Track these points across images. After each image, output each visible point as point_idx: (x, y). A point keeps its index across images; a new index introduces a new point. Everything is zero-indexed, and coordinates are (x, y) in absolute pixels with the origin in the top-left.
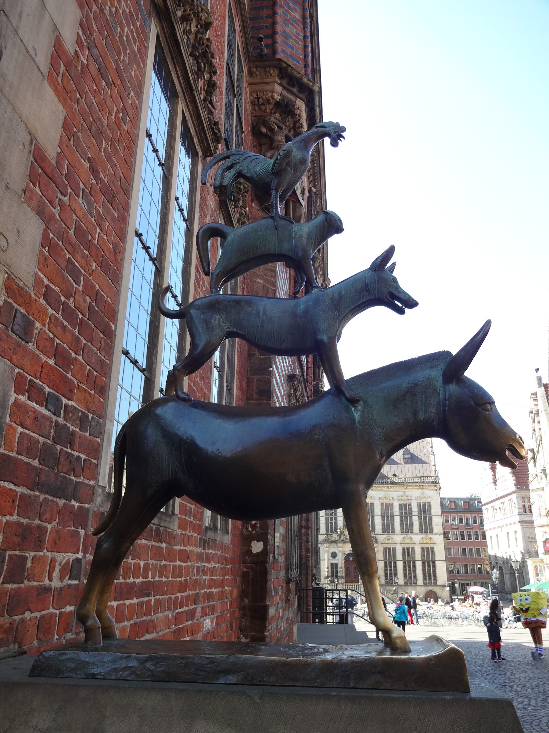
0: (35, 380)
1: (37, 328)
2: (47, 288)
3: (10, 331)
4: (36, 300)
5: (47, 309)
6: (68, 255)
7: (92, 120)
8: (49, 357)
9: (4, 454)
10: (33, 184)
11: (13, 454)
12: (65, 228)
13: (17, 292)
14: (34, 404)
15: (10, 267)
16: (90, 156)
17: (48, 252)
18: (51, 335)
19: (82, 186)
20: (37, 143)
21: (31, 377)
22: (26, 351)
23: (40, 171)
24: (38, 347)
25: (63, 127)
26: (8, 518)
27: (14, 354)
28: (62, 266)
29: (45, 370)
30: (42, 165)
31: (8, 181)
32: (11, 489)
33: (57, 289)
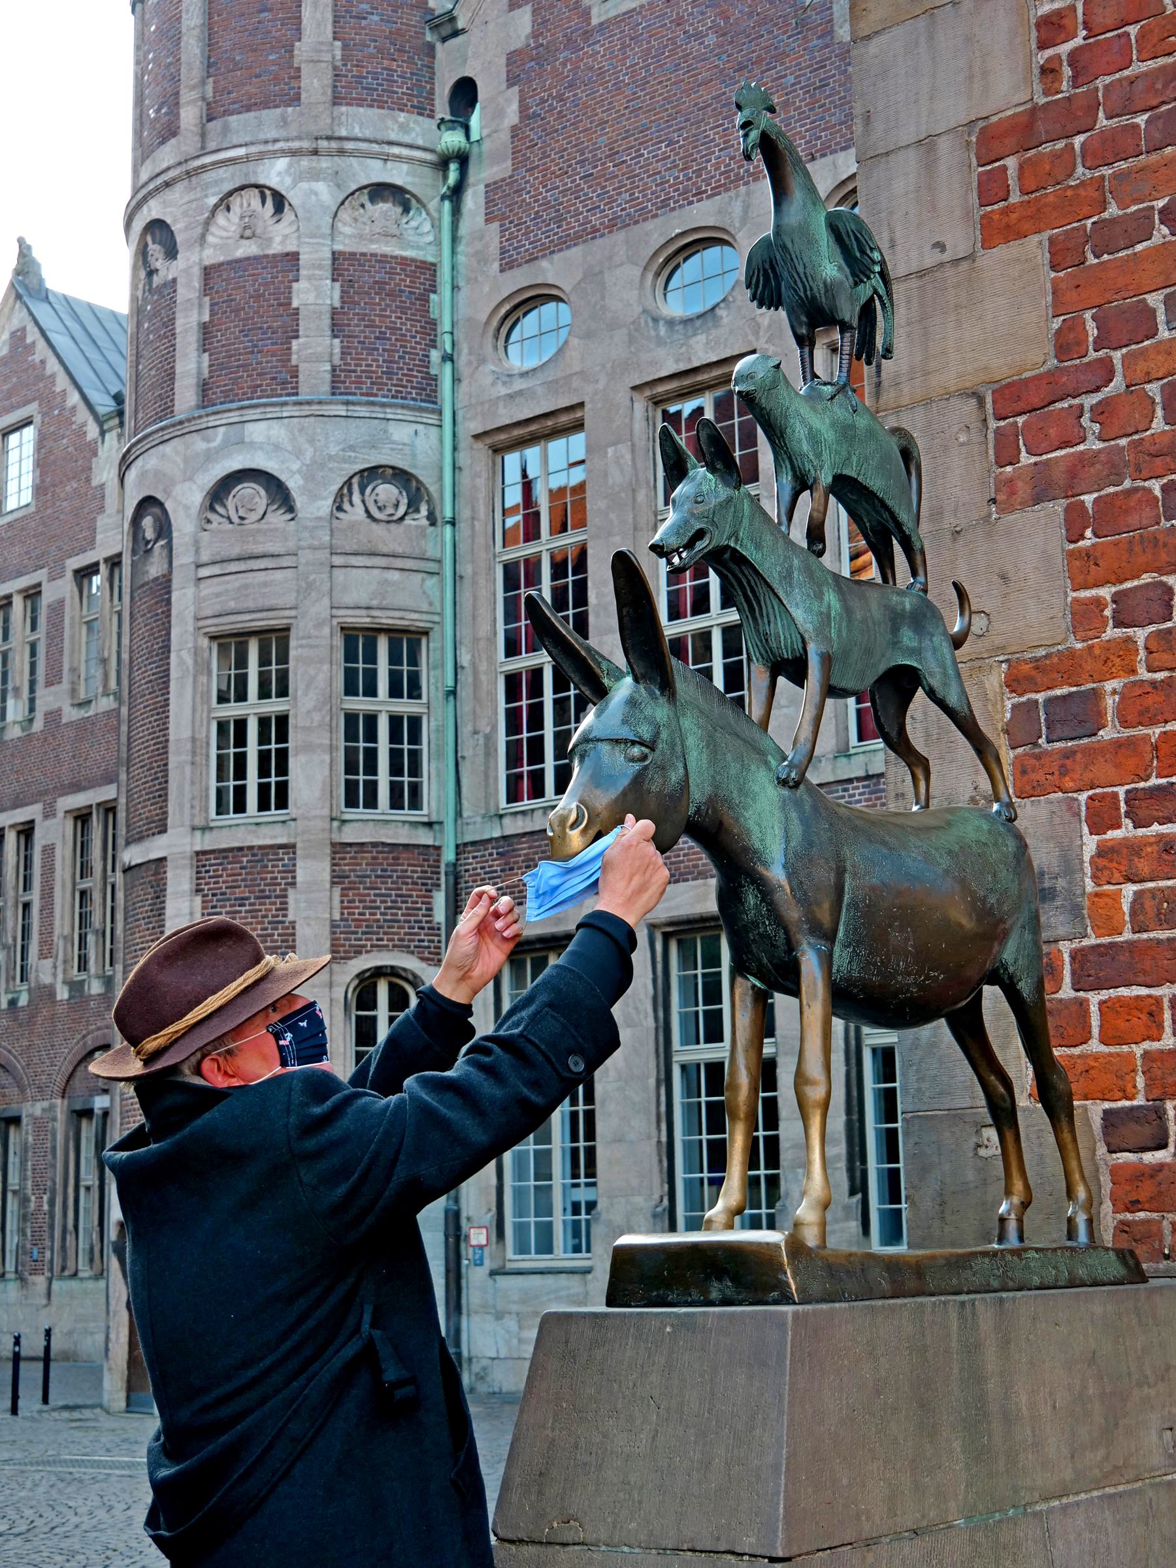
0: (1142, 785)
1: (1114, 692)
2: (1114, 602)
3: (1045, 746)
4: (1091, 648)
5: (1129, 640)
6: (1156, 486)
7: (1141, 120)
8: (1166, 722)
9: (1099, 946)
10: (1011, 464)
11: (1127, 935)
12: (1129, 443)
13: (1033, 673)
14: (1156, 828)
15: (1004, 648)
16: (1160, 204)
17: (1096, 535)
18: (1160, 676)
19: (1155, 300)
20: (996, 386)
21: (1127, 787)
22: (1091, 753)
23: (1020, 420)
24: (1125, 724)
25: (1054, 267)
26: (1146, 1045)
27: (1064, 771)
28: (1145, 522)
29: (1165, 749)
30: (1020, 406)
31: (954, 522)
32: (1138, 997)
33: (1146, 578)
